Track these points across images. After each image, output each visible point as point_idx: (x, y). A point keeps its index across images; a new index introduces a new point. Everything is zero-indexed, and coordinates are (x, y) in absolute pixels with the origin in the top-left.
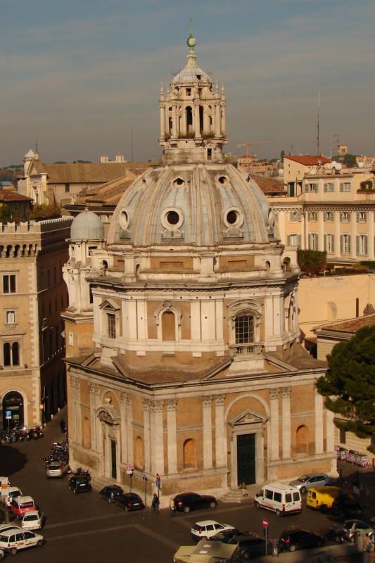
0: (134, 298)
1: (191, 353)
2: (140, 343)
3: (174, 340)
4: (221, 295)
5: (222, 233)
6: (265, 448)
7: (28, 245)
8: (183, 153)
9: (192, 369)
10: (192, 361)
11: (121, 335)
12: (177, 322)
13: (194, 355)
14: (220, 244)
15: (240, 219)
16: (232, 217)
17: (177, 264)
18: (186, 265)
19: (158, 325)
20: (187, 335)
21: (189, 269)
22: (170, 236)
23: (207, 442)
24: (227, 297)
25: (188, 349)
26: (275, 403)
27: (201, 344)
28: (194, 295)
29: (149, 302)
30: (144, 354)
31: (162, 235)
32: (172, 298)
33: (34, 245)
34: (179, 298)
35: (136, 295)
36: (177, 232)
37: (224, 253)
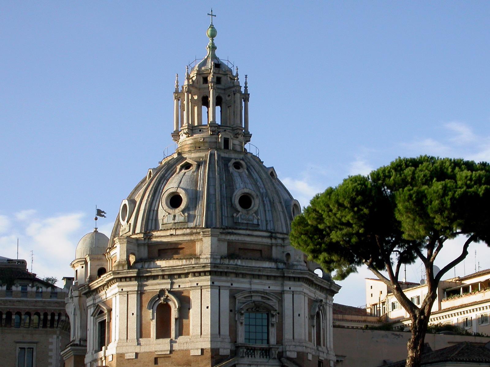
1: (188, 351)
2: (130, 344)
4: (227, 281)
5: (233, 217)
7: (49, 313)
12: (174, 314)
13: (193, 353)
14: (227, 228)
15: (256, 204)
16: (246, 201)
18: (187, 251)
21: (191, 255)
24: (235, 285)
25: (185, 347)
27: (201, 339)
33: (56, 314)
35: (127, 286)
37: (232, 238)
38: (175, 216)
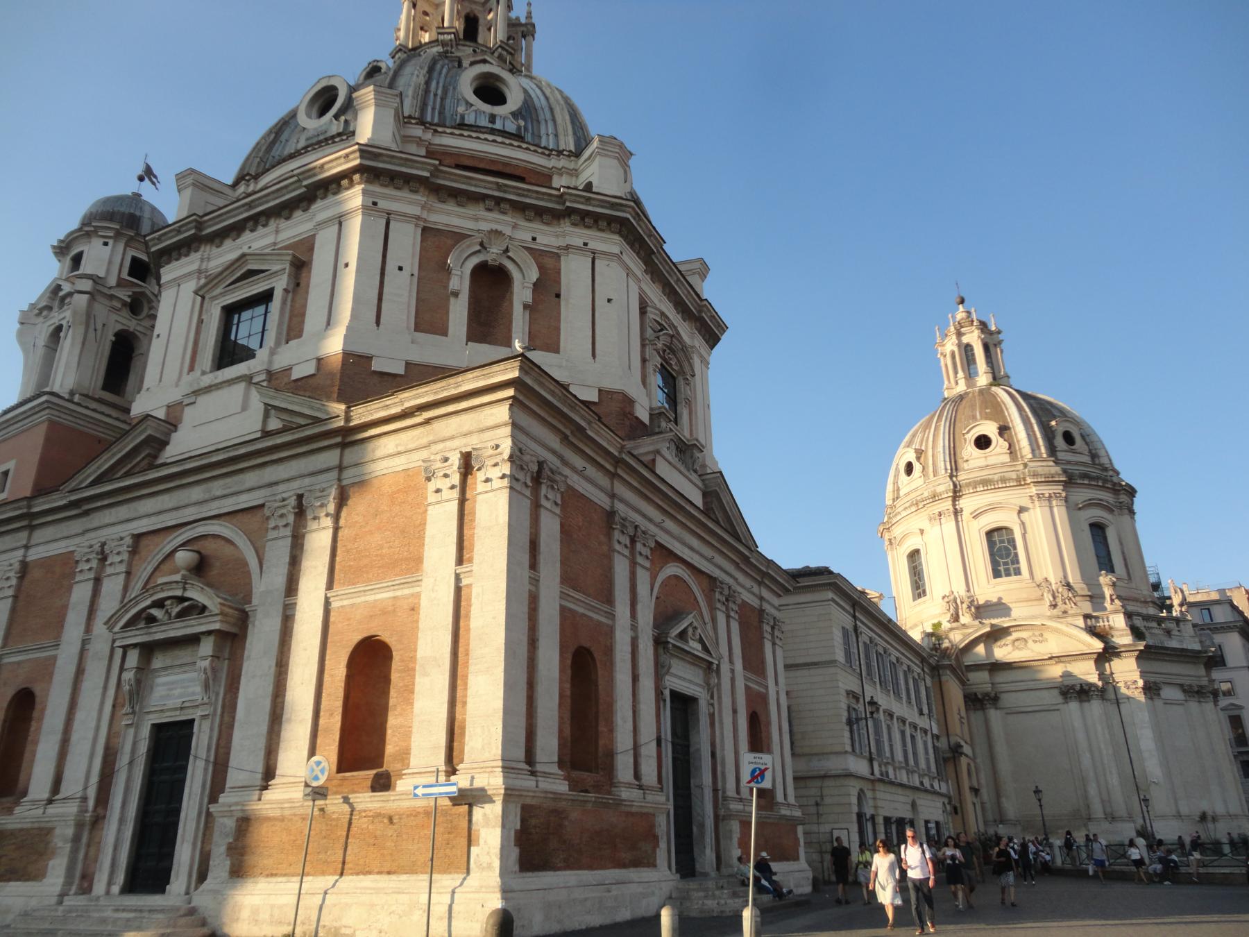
0: (382, 204)
6: (713, 755)
12: (521, 293)
26: (721, 618)
28: (575, 235)
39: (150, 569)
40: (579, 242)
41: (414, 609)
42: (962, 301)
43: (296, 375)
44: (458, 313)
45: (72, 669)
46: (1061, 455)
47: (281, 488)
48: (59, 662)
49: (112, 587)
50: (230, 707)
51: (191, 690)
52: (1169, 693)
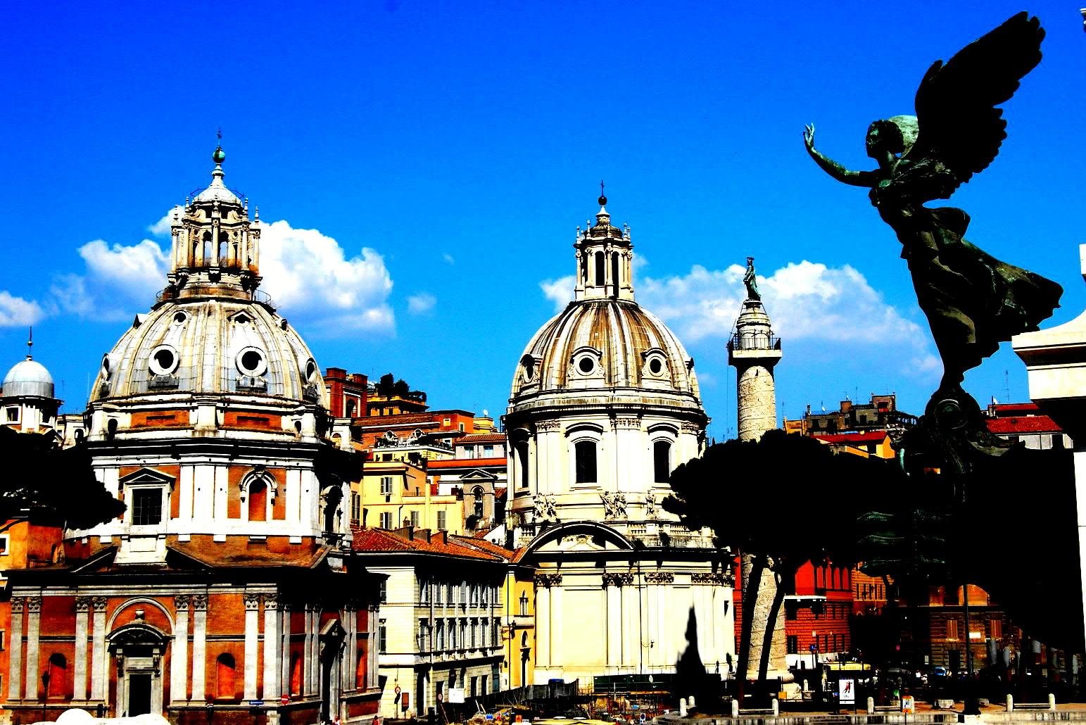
3: (264, 519)
8: (225, 288)
9: (288, 560)
10: (288, 549)
11: (175, 514)
12: (270, 495)
13: (292, 540)
17: (263, 420)
18: (273, 423)
19: (243, 499)
20: (280, 514)
22: (249, 384)
23: (306, 659)
29: (228, 466)
30: (223, 539)
31: (239, 383)
32: (263, 462)
34: (272, 463)
36: (259, 380)
38: (253, 381)
39: (117, 612)
40: (294, 464)
41: (242, 648)
42: (603, 201)
43: (181, 538)
44: (244, 508)
45: (85, 650)
46: (645, 384)
47: (181, 590)
48: (77, 645)
49: (99, 618)
50: (168, 672)
51: (147, 663)
52: (678, 579)
